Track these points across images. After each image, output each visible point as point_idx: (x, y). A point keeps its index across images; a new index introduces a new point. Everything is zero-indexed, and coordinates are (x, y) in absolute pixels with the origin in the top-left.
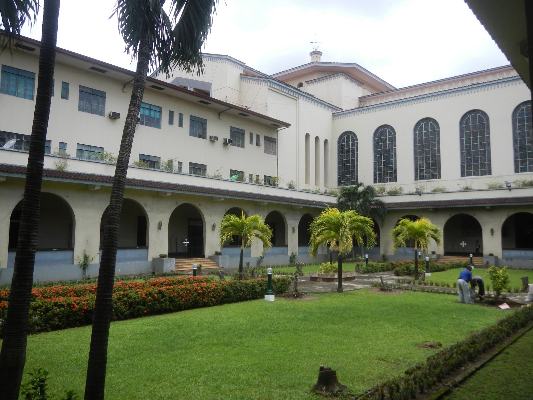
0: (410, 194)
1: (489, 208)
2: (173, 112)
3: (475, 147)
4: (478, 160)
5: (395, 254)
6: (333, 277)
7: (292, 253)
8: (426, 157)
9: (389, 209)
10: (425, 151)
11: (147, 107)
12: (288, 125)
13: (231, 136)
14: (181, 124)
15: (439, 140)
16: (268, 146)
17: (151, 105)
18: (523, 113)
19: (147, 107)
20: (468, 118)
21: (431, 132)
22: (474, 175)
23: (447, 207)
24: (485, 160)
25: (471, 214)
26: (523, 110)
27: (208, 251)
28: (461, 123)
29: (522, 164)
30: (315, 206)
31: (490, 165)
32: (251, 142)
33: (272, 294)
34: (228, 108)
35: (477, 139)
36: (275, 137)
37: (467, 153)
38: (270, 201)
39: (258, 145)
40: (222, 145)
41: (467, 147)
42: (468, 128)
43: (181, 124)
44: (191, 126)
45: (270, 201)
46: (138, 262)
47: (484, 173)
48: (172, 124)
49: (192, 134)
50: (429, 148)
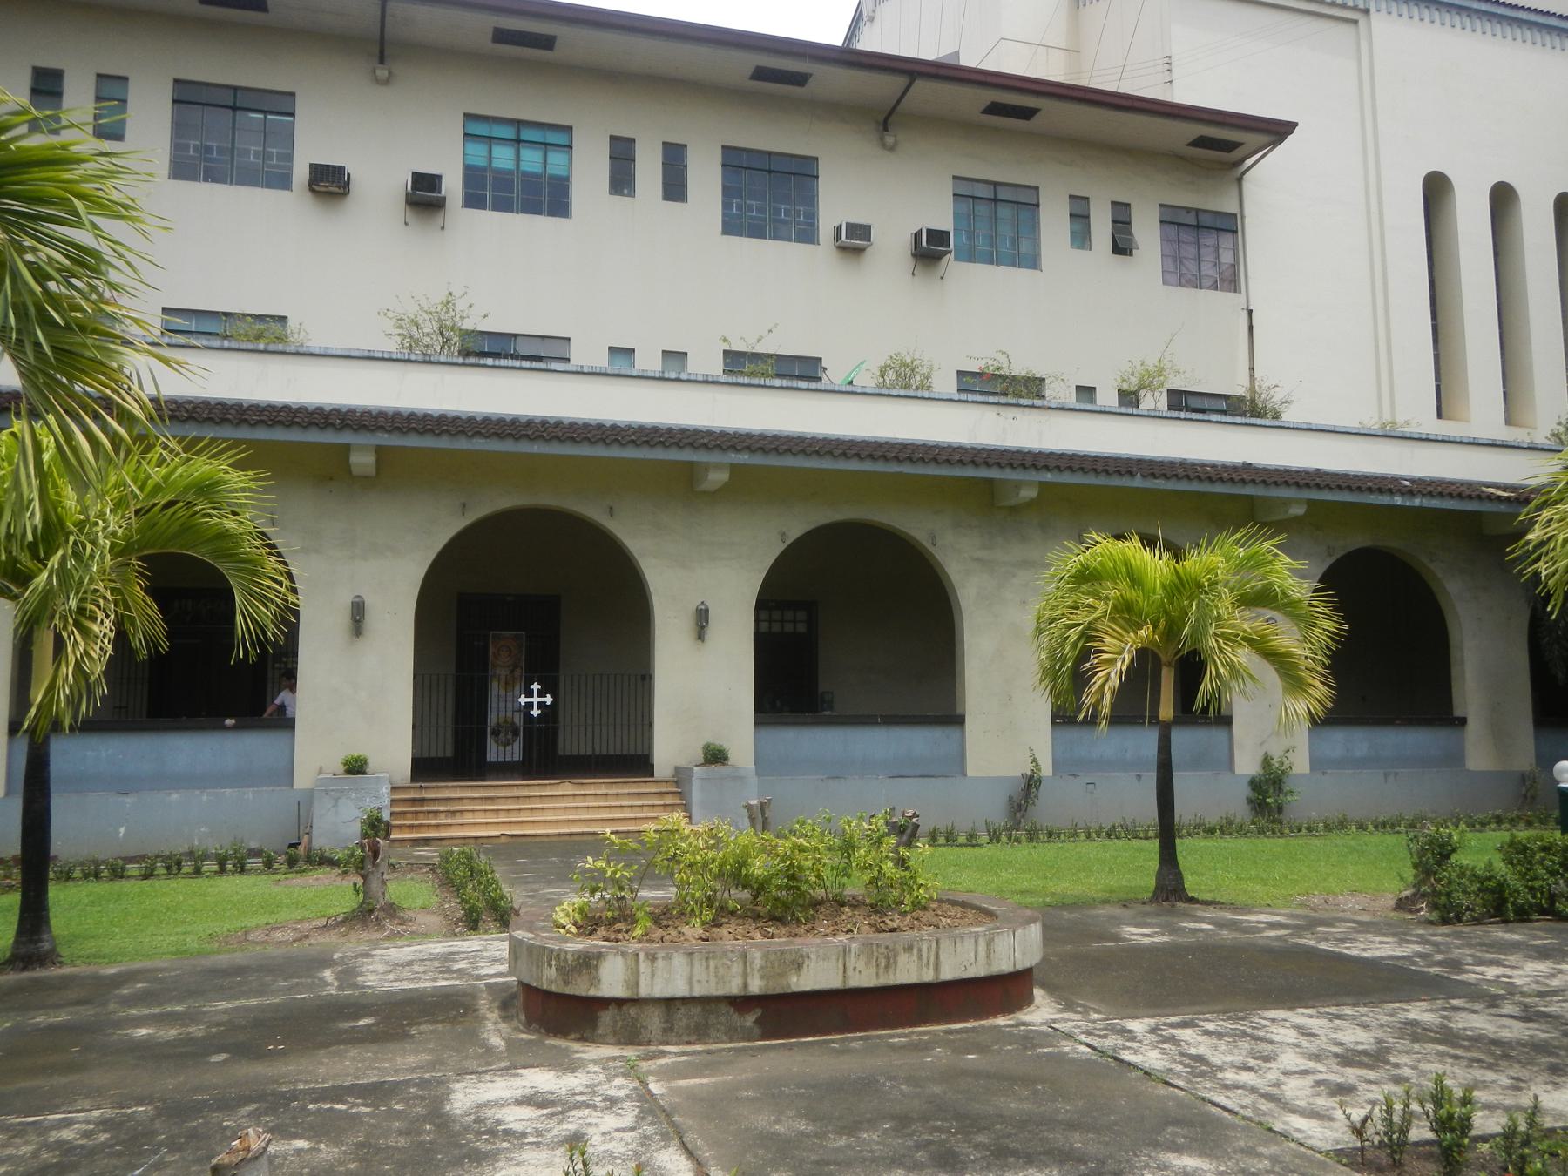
2: (631, 141)
6: (580, 988)
7: (1267, 761)
12: (1278, 131)
13: (956, 215)
14: (675, 188)
16: (1189, 251)
17: (519, 124)
19: (508, 132)
27: (670, 745)
30: (1398, 501)
32: (1081, 236)
34: (901, 81)
36: (1231, 207)
38: (1048, 477)
39: (1122, 247)
40: (910, 262)
43: (675, 188)
44: (727, 192)
45: (1048, 477)
48: (632, 194)
49: (731, 226)
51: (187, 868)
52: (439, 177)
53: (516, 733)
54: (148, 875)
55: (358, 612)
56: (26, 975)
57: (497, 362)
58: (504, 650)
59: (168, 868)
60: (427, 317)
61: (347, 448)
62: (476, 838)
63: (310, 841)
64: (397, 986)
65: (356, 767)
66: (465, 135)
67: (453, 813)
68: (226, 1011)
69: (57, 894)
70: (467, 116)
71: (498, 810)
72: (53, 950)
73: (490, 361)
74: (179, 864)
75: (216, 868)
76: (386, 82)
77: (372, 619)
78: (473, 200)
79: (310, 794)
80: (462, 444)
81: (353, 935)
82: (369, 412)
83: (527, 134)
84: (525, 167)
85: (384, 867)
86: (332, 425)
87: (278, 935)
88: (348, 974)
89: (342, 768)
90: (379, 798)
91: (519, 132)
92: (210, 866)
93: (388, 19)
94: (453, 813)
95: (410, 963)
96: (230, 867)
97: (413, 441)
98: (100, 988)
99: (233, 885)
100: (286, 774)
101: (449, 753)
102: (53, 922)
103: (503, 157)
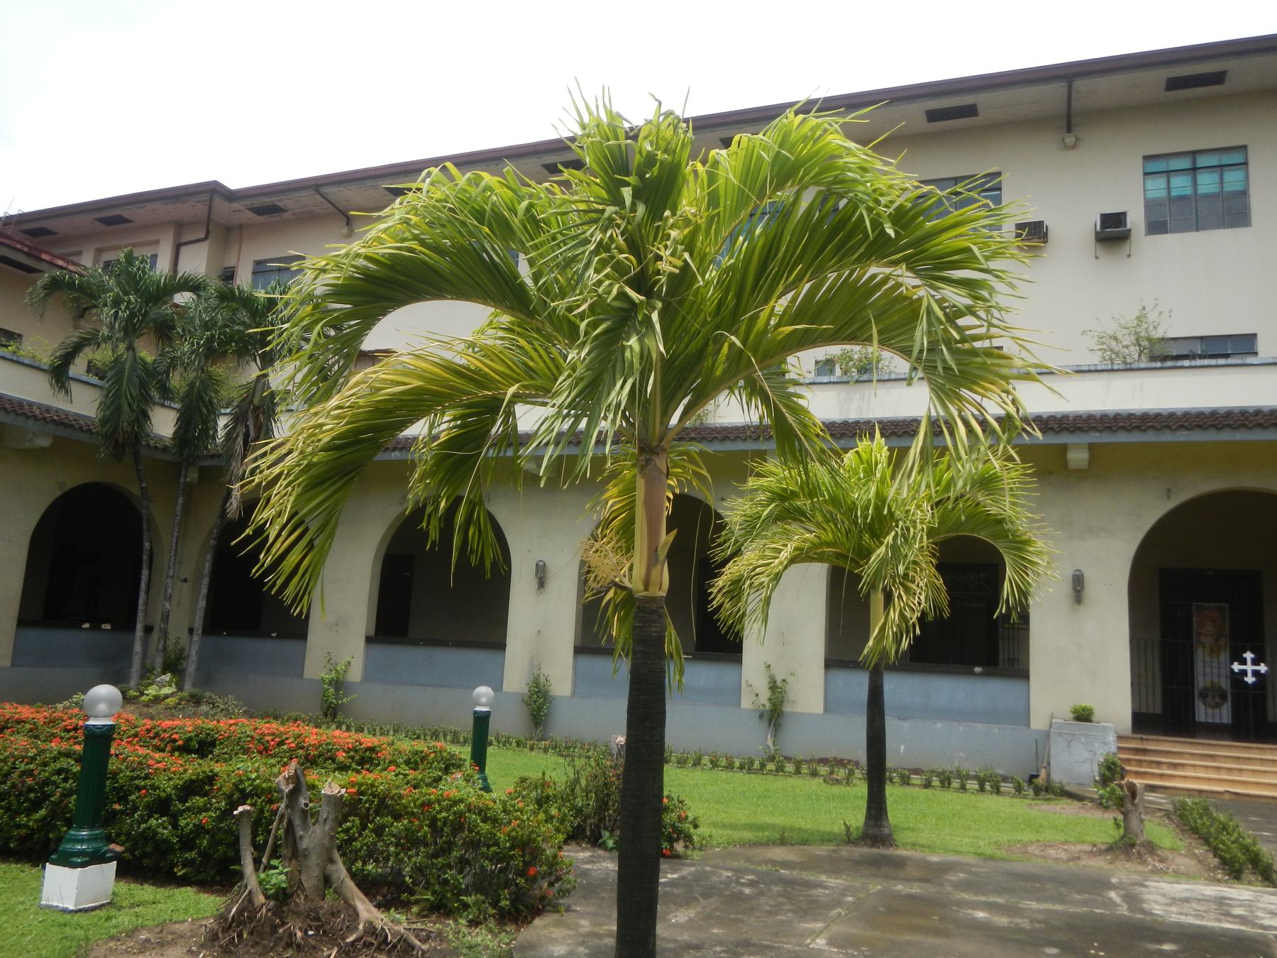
11: (1185, 163)
17: (1194, 154)
19: (1185, 163)
33: (66, 861)
46: (979, 726)
51: (956, 783)
52: (1124, 214)
53: (1223, 697)
54: (927, 785)
55: (1078, 583)
56: (875, 850)
57: (1194, 363)
58: (1208, 623)
59: (942, 782)
60: (1126, 332)
61: (1064, 448)
62: (1200, 791)
63: (1048, 774)
64: (1183, 919)
65: (1083, 716)
66: (1145, 174)
67: (1175, 766)
68: (1040, 911)
69: (892, 792)
70: (1146, 158)
71: (1218, 768)
72: (890, 836)
73: (1186, 363)
74: (949, 779)
75: (977, 787)
76: (1074, 146)
77: (1091, 590)
78: (1156, 227)
79: (1047, 735)
80: (1167, 437)
81: (1119, 864)
82: (1106, 415)
83: (1202, 161)
84: (1202, 190)
85: (1141, 809)
86: (1052, 429)
87: (1052, 852)
88: (1133, 900)
89: (1072, 715)
90: (1107, 746)
91: (1194, 163)
92: (972, 785)
93: (1074, 95)
94: (1175, 766)
95: (1187, 900)
96: (988, 787)
97: (1121, 437)
98: (933, 873)
99: (989, 802)
100: (1024, 717)
101: (1159, 711)
102: (889, 815)
103: (1181, 184)
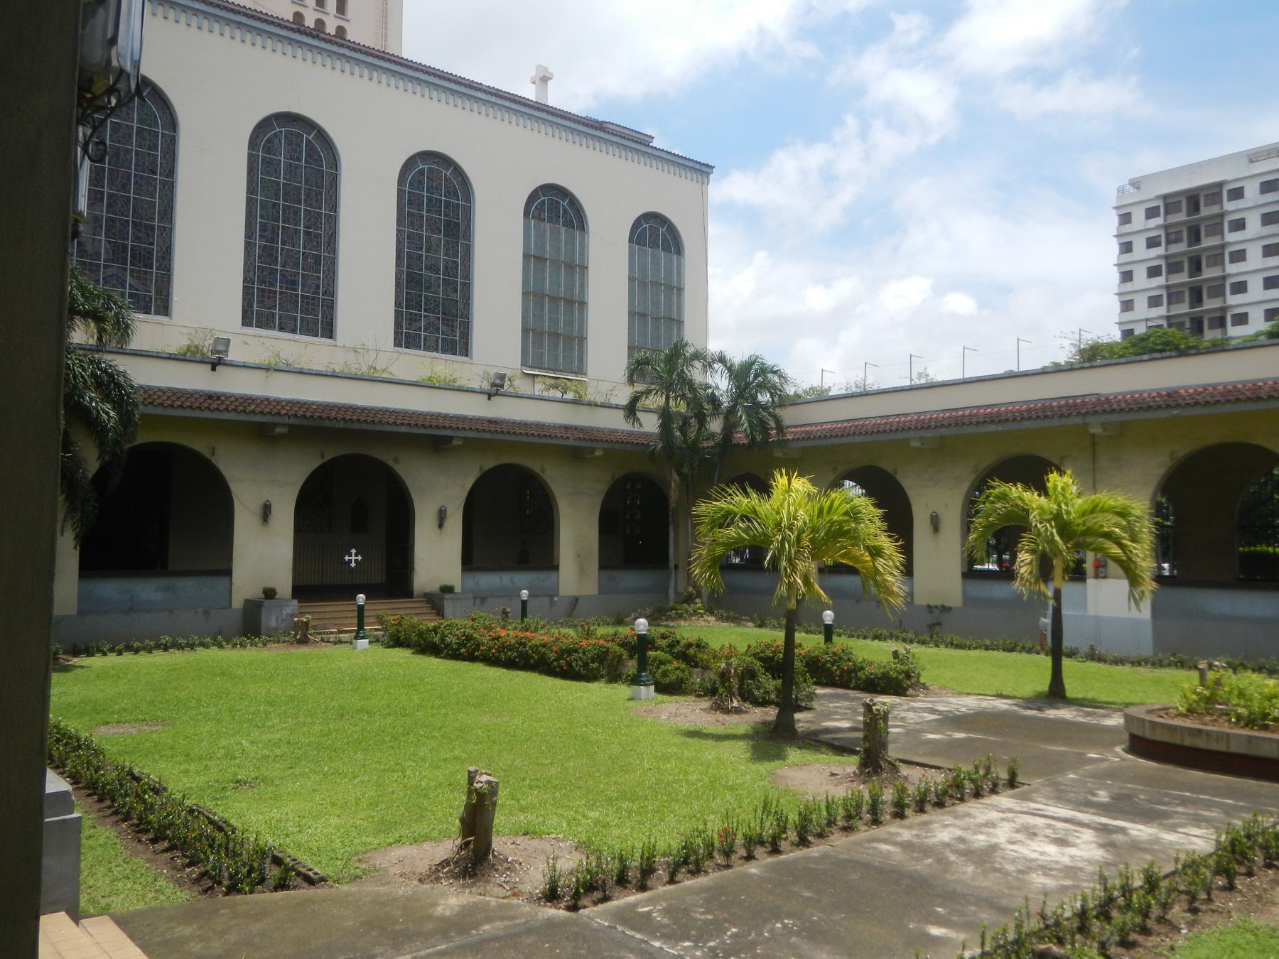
0: (171, 358)
1: (460, 443)
3: (291, 237)
4: (294, 283)
5: (82, 613)
8: (111, 221)
9: (150, 410)
10: (111, 196)
15: (171, 172)
18: (421, 183)
20: (275, 135)
21: (140, 131)
22: (281, 329)
23: (349, 426)
24: (318, 287)
25: (384, 455)
26: (421, 172)
28: (253, 143)
29: (409, 324)
31: (330, 306)
35: (297, 212)
37: (264, 248)
41: (264, 228)
42: (271, 166)
47: (310, 330)
50: (125, 187)
